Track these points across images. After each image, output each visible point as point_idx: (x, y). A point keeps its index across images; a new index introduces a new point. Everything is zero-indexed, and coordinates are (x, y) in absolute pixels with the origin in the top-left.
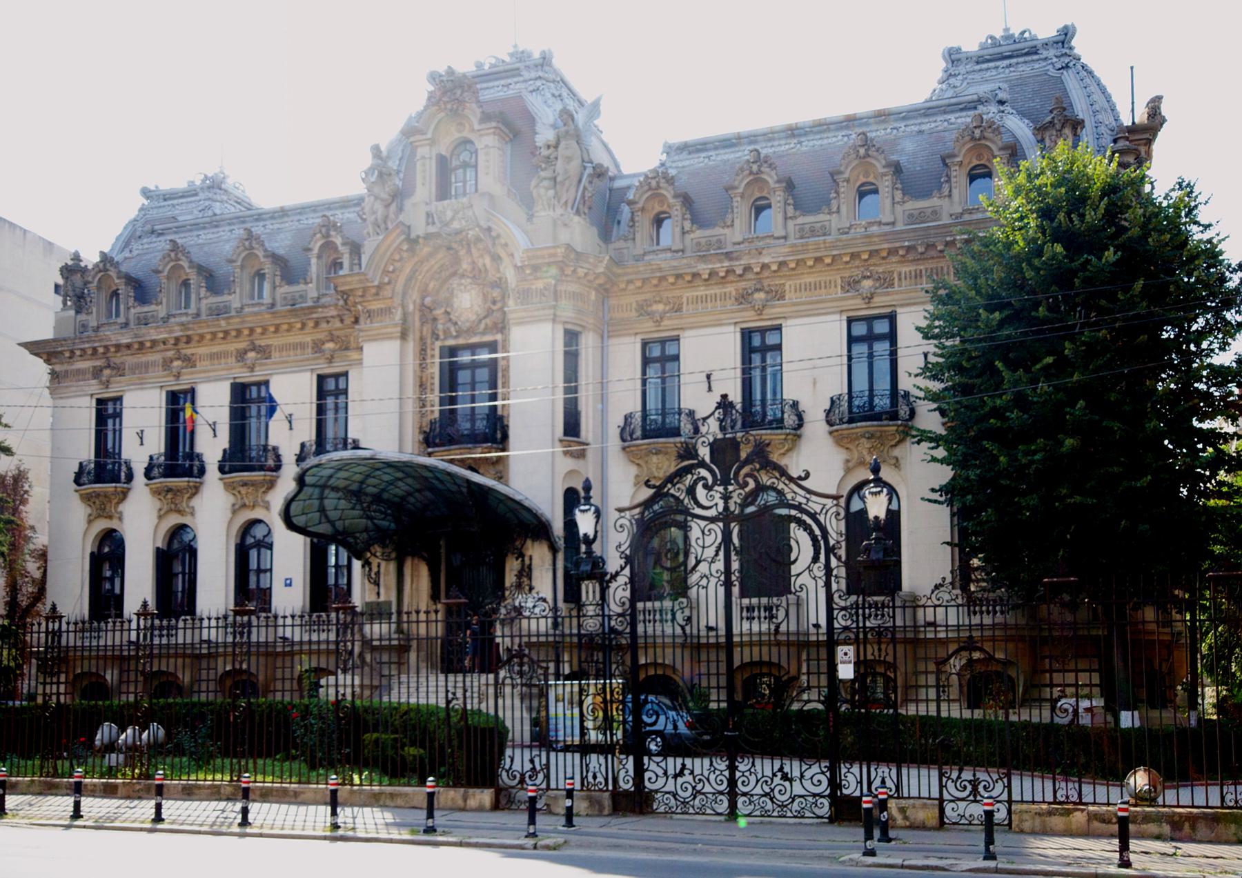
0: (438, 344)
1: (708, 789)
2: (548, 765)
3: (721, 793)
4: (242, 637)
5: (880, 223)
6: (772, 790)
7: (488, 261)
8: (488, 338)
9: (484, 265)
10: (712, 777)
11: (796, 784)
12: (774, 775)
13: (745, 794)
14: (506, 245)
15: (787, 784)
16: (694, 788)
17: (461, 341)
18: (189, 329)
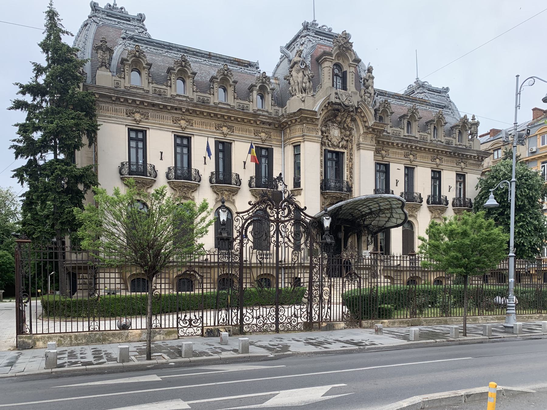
0: (324, 148)
1: (268, 322)
2: (202, 317)
3: (273, 323)
4: (413, 264)
5: (441, 141)
6: (291, 321)
7: (349, 120)
8: (342, 150)
9: (345, 121)
10: (270, 318)
11: (299, 319)
12: (292, 316)
13: (281, 323)
14: (363, 117)
15: (296, 319)
16: (263, 322)
17: (332, 149)
18: (198, 107)
